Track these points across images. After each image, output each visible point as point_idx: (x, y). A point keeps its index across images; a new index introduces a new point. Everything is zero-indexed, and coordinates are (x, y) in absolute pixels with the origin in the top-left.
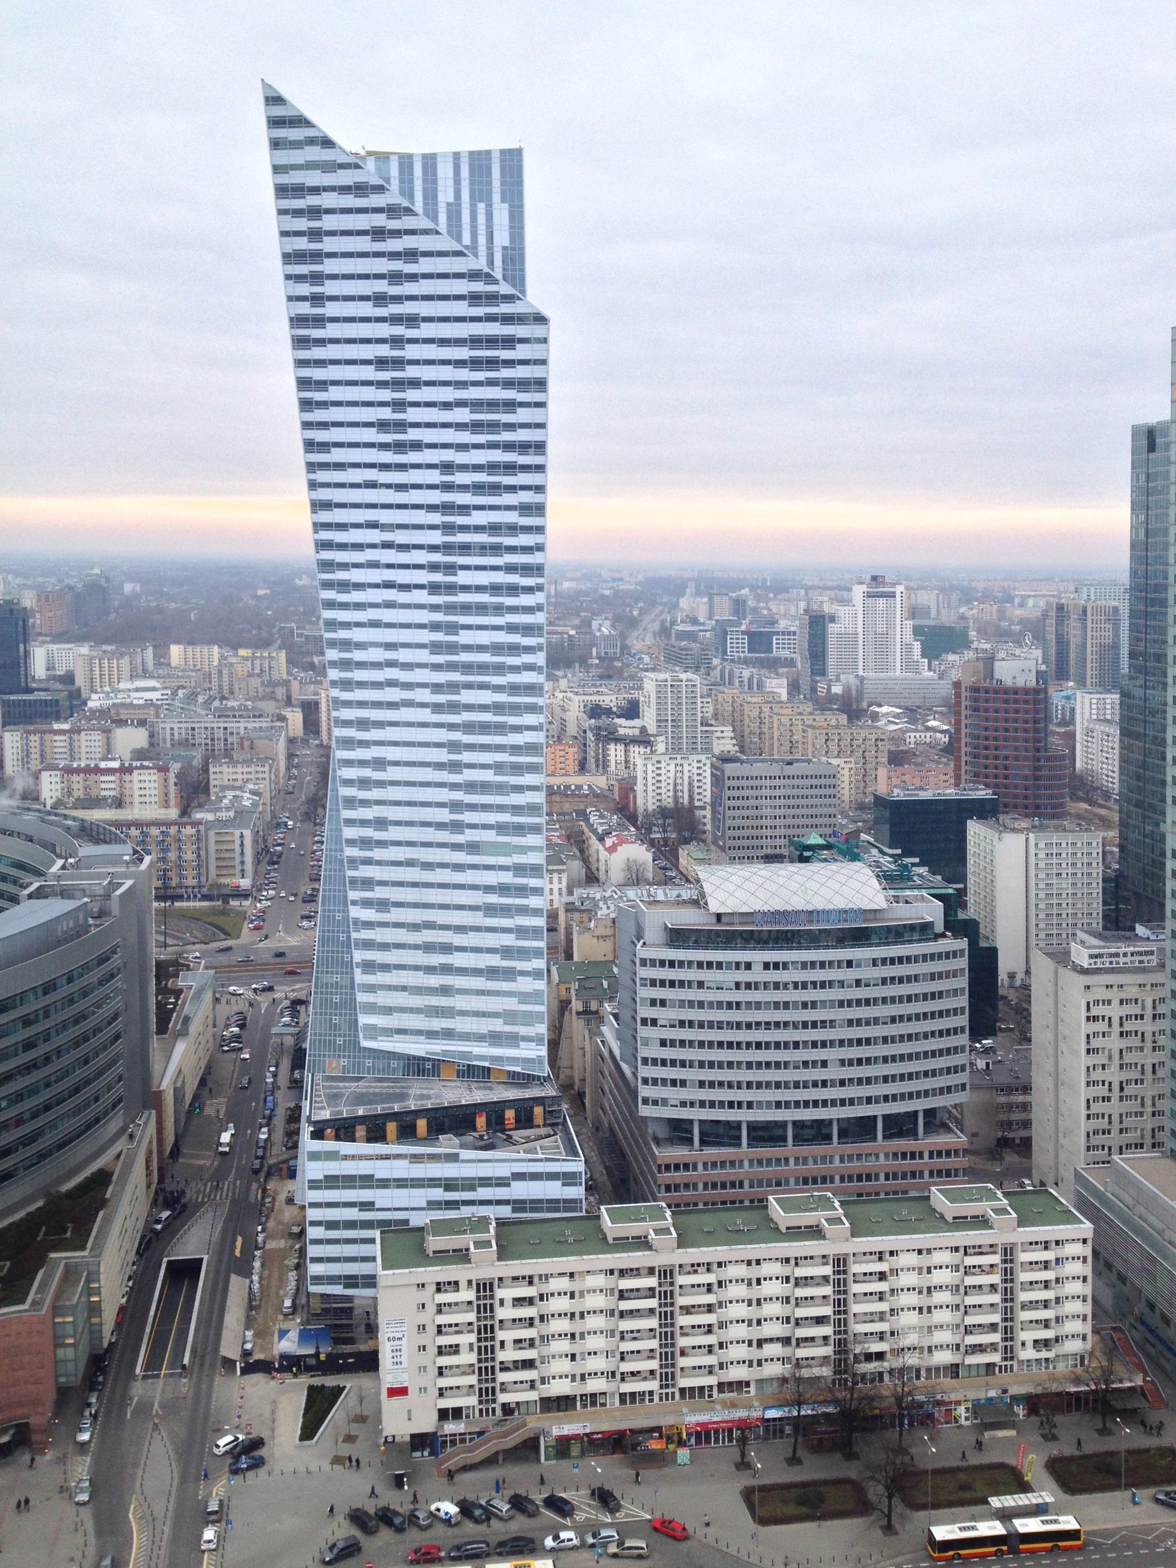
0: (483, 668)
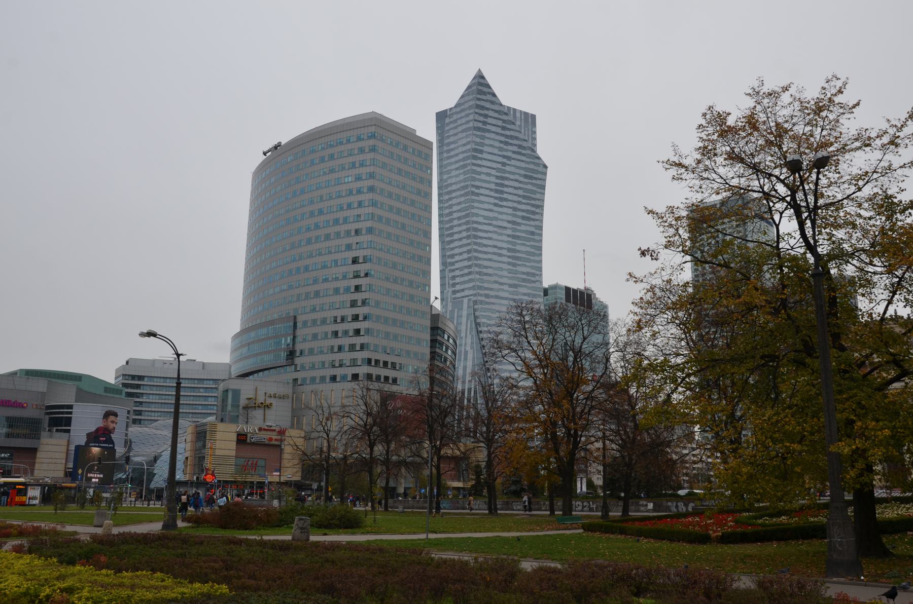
0: (524, 280)
